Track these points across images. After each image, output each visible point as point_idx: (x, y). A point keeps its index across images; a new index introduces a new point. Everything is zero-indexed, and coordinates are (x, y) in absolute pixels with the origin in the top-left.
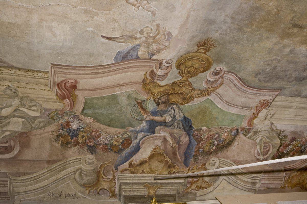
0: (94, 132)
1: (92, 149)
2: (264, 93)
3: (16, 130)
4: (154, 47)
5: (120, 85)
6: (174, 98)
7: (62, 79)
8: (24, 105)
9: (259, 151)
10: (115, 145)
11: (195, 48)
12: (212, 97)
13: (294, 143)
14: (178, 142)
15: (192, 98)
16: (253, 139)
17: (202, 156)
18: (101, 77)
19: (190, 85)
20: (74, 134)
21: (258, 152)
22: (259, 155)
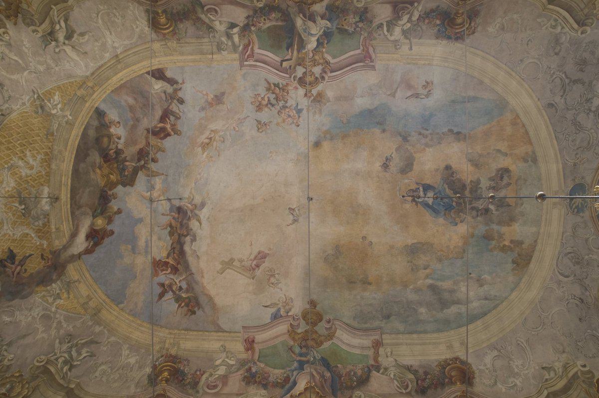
0: (266, 373)
1: (265, 386)
2: (370, 333)
3: (222, 374)
4: (287, 307)
5: (277, 337)
6: (311, 343)
7: (247, 336)
8: (227, 357)
9: (398, 385)
10: (280, 383)
11: (308, 306)
12: (335, 341)
13: (429, 376)
14: (323, 376)
15: (322, 343)
16: (387, 375)
17: (347, 390)
18: (266, 332)
19: (316, 332)
20: (253, 376)
21: (397, 387)
22: (400, 389)
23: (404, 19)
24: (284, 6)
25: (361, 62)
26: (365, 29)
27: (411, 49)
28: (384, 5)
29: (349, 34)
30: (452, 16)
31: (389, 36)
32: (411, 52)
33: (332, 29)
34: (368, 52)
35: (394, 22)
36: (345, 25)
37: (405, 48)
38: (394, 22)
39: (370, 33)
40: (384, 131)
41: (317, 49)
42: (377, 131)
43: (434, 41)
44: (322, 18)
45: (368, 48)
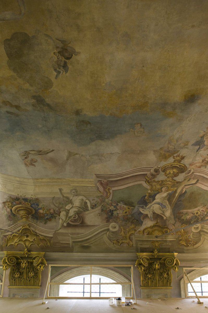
23: (73, 212)
24: (178, 224)
25: (112, 181)
26: (108, 205)
27: (60, 190)
28: (93, 224)
29: (122, 201)
30: (30, 216)
31: (84, 199)
32: (60, 187)
33: (138, 206)
34: (105, 189)
35: (81, 210)
36: (127, 209)
37: (66, 190)
38: (81, 210)
39: (103, 201)
40: (78, 113)
41: (156, 192)
42: (88, 113)
43: (39, 196)
44: (147, 216)
45: (104, 190)
